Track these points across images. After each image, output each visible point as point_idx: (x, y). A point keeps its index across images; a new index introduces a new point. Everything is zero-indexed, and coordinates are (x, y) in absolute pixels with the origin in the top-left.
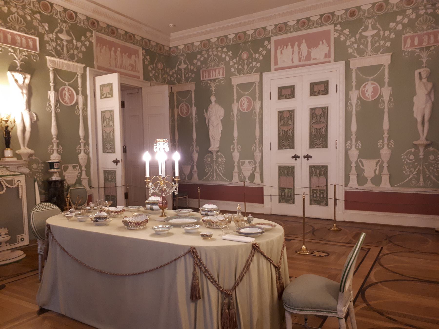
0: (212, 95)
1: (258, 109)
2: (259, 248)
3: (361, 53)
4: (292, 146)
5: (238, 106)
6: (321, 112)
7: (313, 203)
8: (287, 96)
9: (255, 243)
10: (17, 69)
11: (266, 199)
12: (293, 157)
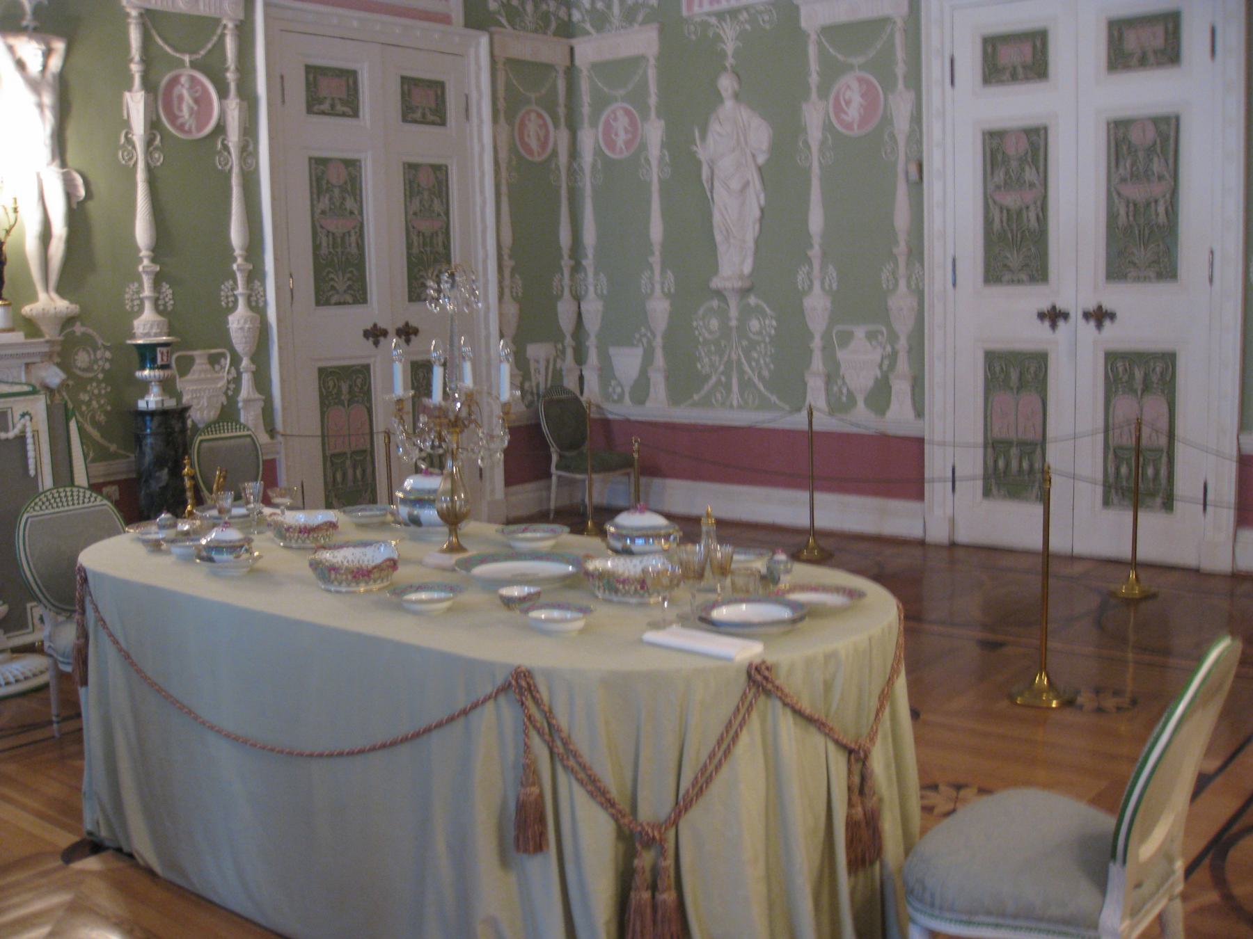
0: (725, 69)
1: (902, 125)
2: (772, 682)
4: (1038, 272)
5: (827, 114)
7: (1114, 498)
8: (1020, 70)
9: (757, 661)
10: (25, 23)
12: (1041, 316)
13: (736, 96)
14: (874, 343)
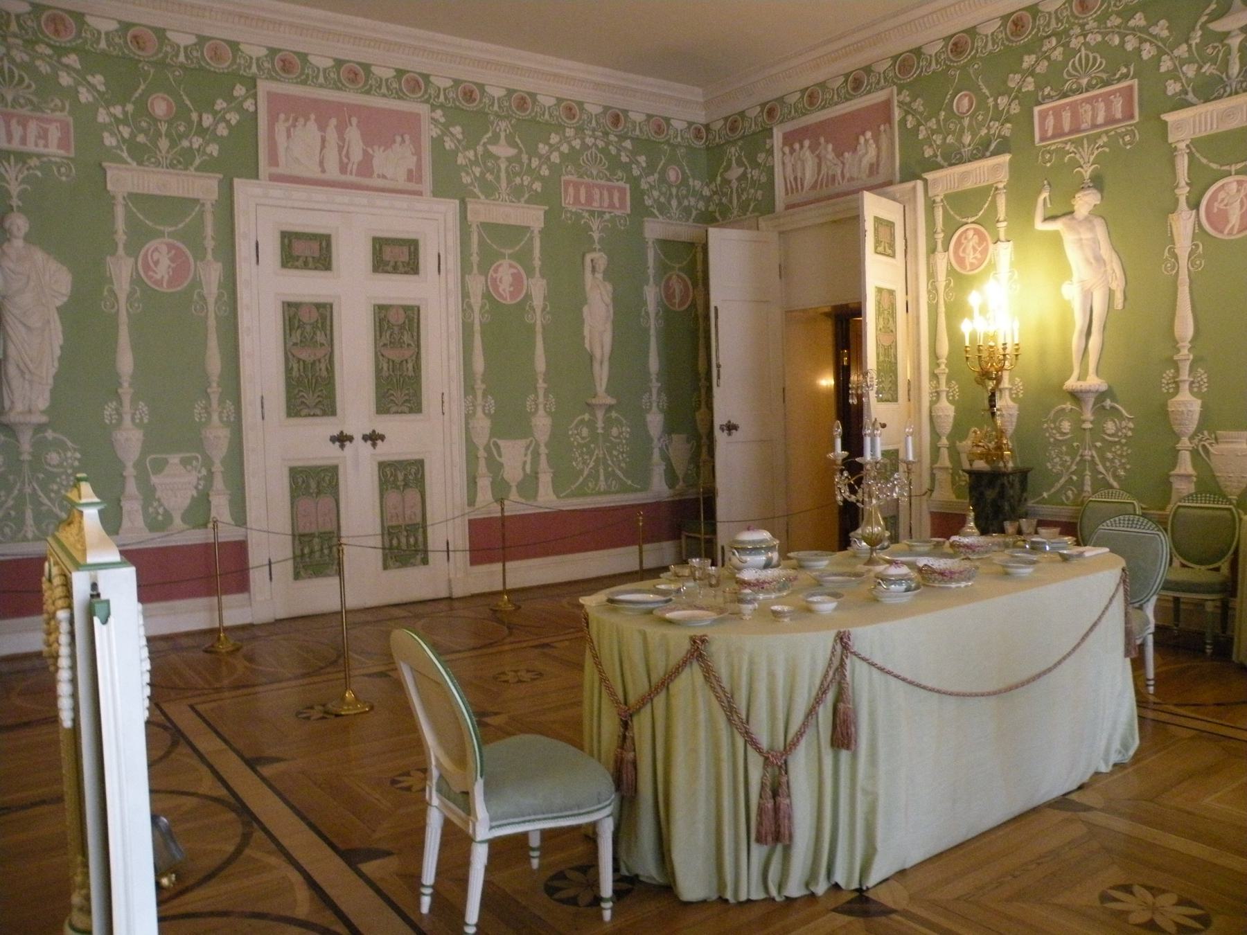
3: (490, 190)
4: (327, 407)
7: (390, 562)
13: (27, 238)
14: (189, 467)
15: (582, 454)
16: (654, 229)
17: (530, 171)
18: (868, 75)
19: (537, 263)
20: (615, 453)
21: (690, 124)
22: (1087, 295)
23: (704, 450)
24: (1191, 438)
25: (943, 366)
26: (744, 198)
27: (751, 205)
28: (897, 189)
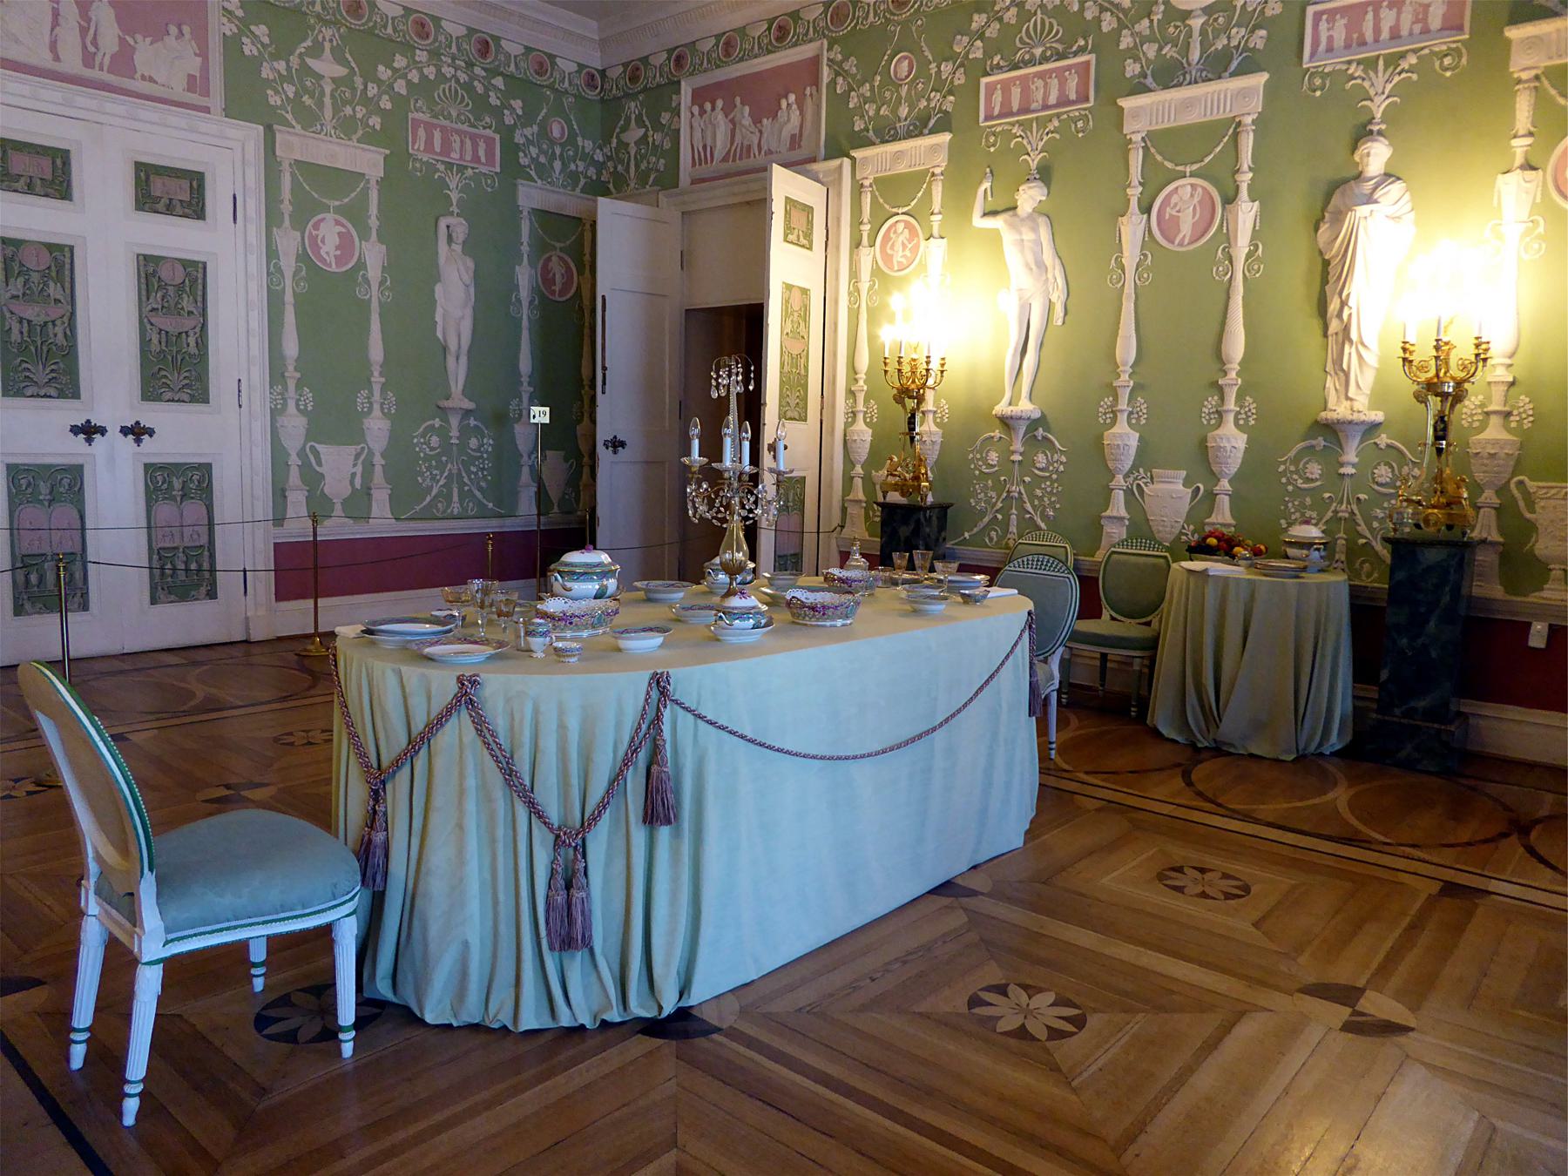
3: (309, 119)
4: (66, 384)
6: (179, 276)
11: (227, 583)
12: (75, 430)
15: (428, 469)
16: (531, 196)
17: (366, 101)
18: (796, 23)
19: (373, 222)
20: (473, 469)
21: (581, 66)
22: (1026, 308)
23: (586, 470)
24: (1126, 476)
25: (861, 383)
26: (643, 166)
27: (649, 175)
28: (820, 167)
